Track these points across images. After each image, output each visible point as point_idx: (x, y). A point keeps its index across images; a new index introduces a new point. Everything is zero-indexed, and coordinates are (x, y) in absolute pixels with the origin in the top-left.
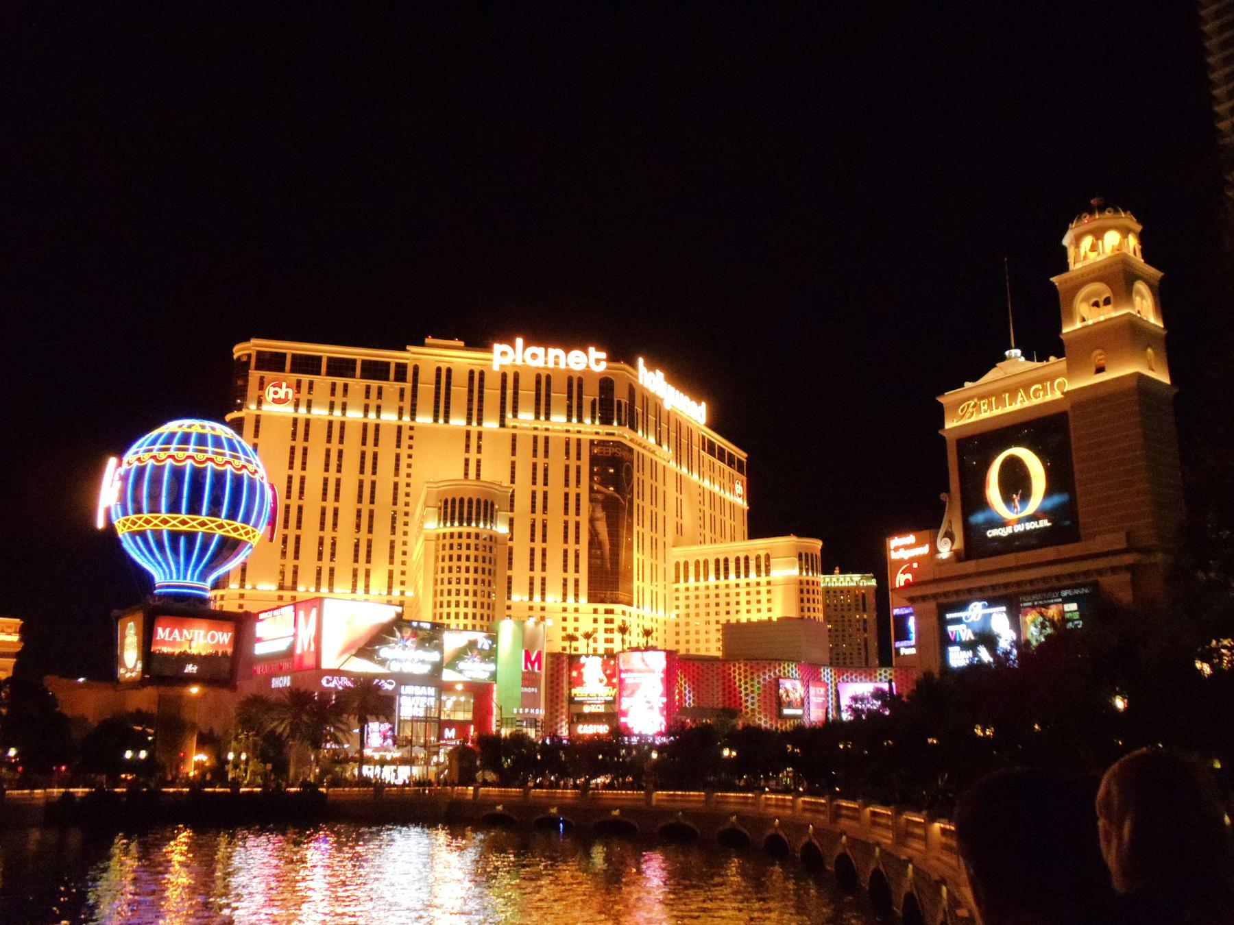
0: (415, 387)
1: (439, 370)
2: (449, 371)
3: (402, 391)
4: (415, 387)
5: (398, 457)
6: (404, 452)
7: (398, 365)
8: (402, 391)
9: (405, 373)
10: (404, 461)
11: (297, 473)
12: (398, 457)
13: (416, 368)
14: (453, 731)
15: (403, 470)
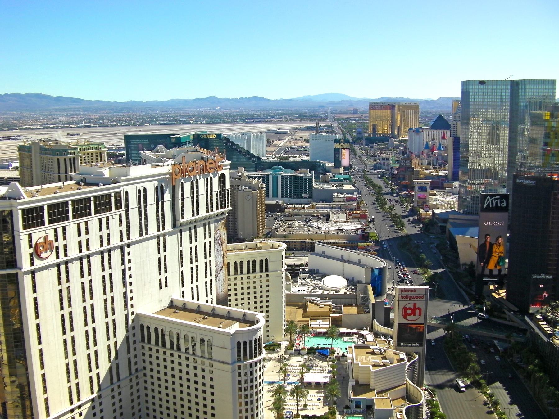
0: (127, 211)
3: (120, 216)
4: (127, 211)
7: (116, 193)
8: (120, 216)
13: (127, 193)
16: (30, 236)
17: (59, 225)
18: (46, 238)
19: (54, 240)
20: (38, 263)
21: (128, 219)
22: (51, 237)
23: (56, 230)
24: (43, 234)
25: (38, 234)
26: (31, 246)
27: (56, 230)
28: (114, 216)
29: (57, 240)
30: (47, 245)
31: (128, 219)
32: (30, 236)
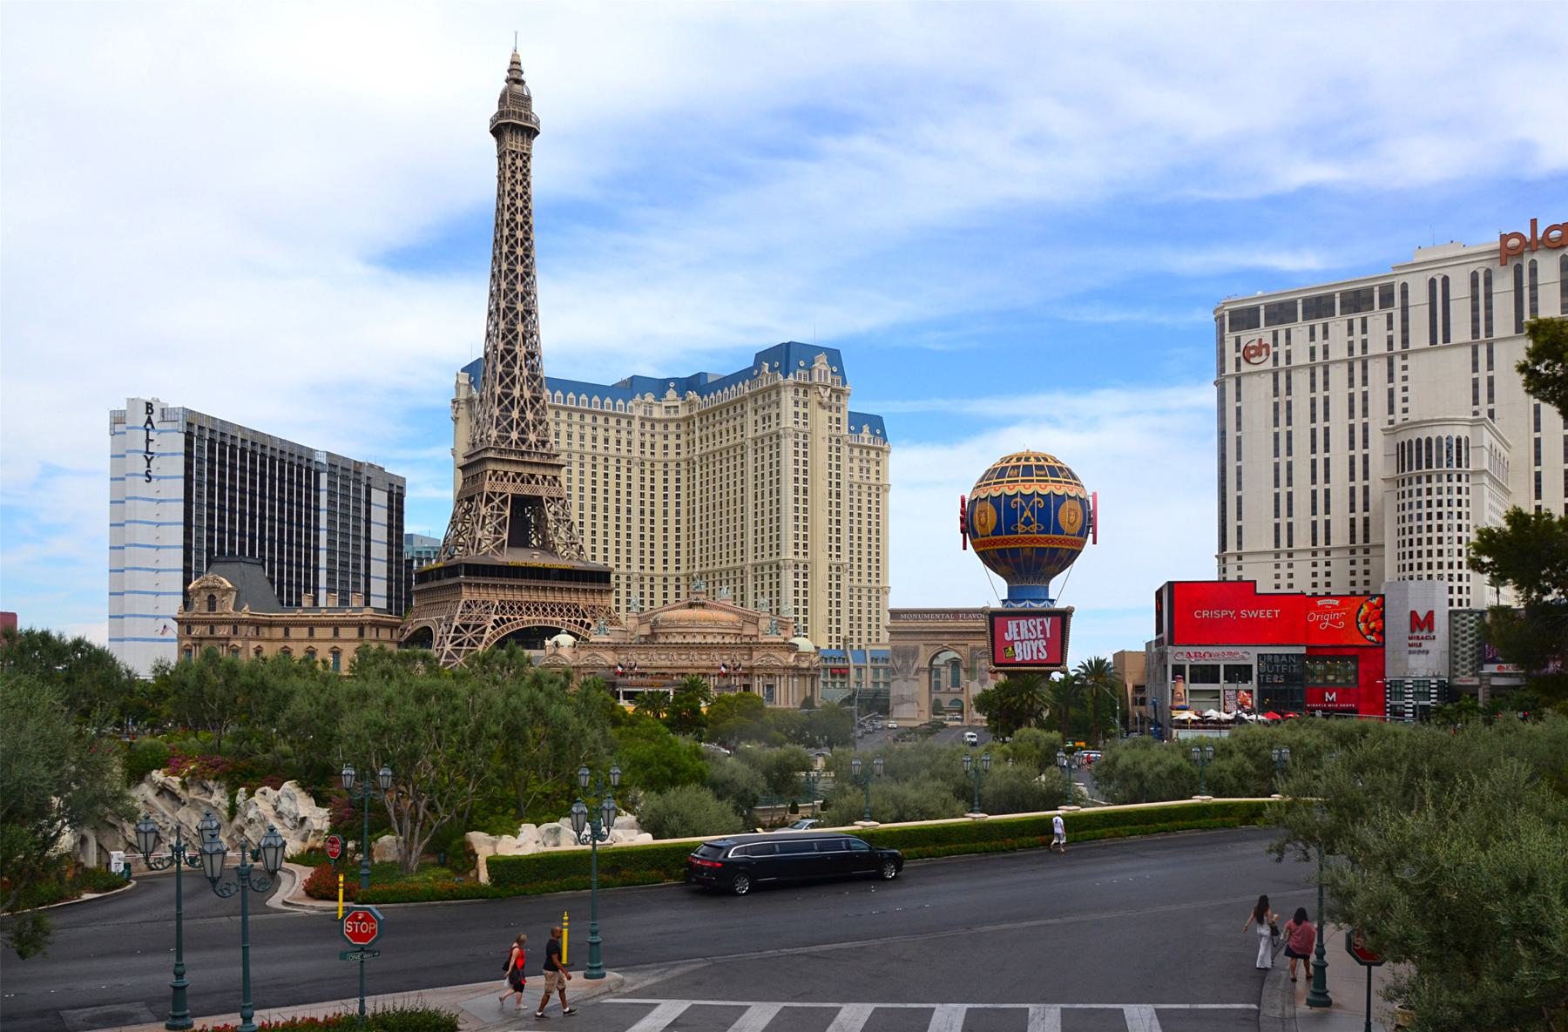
0: (1405, 309)
1: (1432, 282)
2: (1446, 280)
3: (1390, 317)
4: (1405, 309)
5: (1391, 393)
6: (1398, 385)
7: (1382, 288)
8: (1390, 317)
9: (1391, 296)
10: (1398, 395)
11: (1283, 428)
12: (1391, 393)
13: (1404, 287)
14: (1334, 694)
15: (1398, 405)
16: (1238, 340)
17: (1281, 330)
18: (1260, 340)
19: (1271, 345)
20: (1245, 368)
21: (1405, 320)
22: (1268, 340)
23: (1275, 334)
24: (1257, 338)
25: (1248, 337)
26: (1238, 350)
27: (1275, 334)
28: (1377, 319)
29: (1275, 343)
30: (1260, 348)
31: (1405, 320)
32: (1238, 340)
